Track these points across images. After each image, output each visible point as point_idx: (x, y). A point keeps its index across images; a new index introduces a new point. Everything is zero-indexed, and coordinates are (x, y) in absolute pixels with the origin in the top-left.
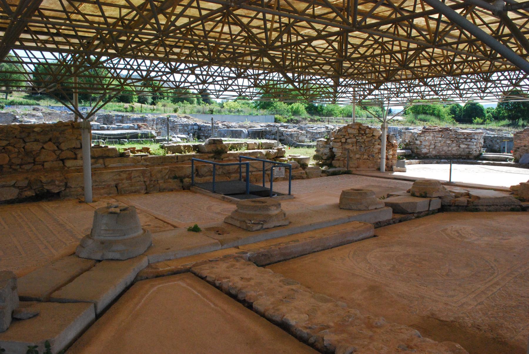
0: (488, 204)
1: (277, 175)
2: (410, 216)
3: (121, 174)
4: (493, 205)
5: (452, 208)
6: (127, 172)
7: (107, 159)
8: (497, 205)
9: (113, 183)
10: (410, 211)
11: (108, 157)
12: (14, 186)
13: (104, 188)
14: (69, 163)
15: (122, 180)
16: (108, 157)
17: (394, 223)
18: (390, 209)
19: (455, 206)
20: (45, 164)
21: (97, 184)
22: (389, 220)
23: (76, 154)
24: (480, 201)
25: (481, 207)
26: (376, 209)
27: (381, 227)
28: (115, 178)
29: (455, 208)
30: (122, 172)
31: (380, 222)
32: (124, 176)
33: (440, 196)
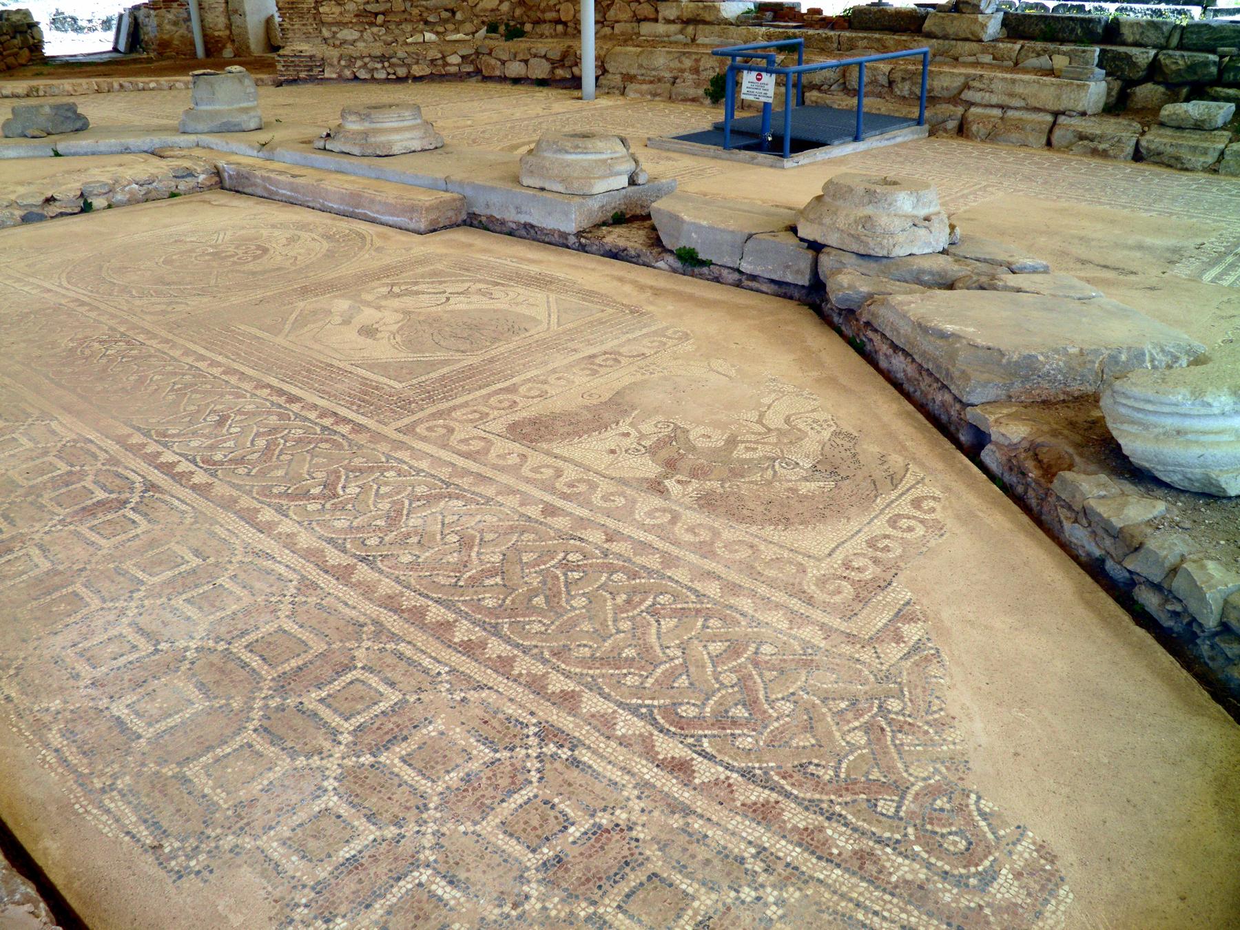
1: (748, 93)
3: (683, 58)
6: (694, 57)
7: (701, 26)
9: (668, 75)
11: (705, 22)
12: (545, 57)
13: (651, 82)
14: (646, 28)
15: (682, 71)
16: (705, 22)
20: (616, 25)
21: (643, 71)
22: (564, 235)
23: (657, 11)
26: (543, 189)
28: (672, 65)
30: (684, 53)
32: (688, 63)
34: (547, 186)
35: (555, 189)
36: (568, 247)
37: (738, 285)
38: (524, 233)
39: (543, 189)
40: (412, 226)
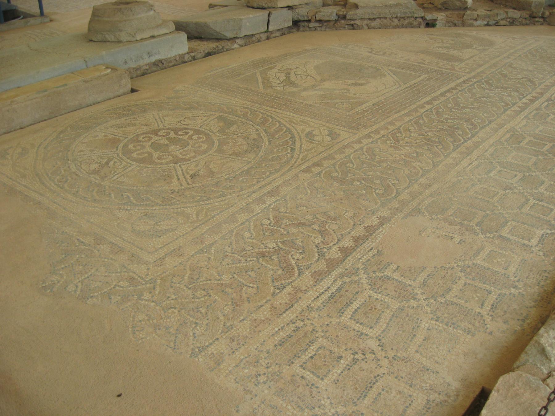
0: (371, 17)
2: (227, 44)
4: (380, 18)
5: (312, 25)
8: (386, 18)
10: (229, 35)
17: (194, 58)
18: (183, 36)
19: (317, 21)
22: (182, 56)
24: (358, 11)
25: (358, 22)
26: (153, 37)
27: (165, 68)
29: (317, 25)
31: (161, 61)
33: (290, 4)
34: (156, 33)
35: (162, 32)
36: (185, 62)
37: (268, 38)
38: (154, 69)
39: (153, 37)
40: (121, 91)
